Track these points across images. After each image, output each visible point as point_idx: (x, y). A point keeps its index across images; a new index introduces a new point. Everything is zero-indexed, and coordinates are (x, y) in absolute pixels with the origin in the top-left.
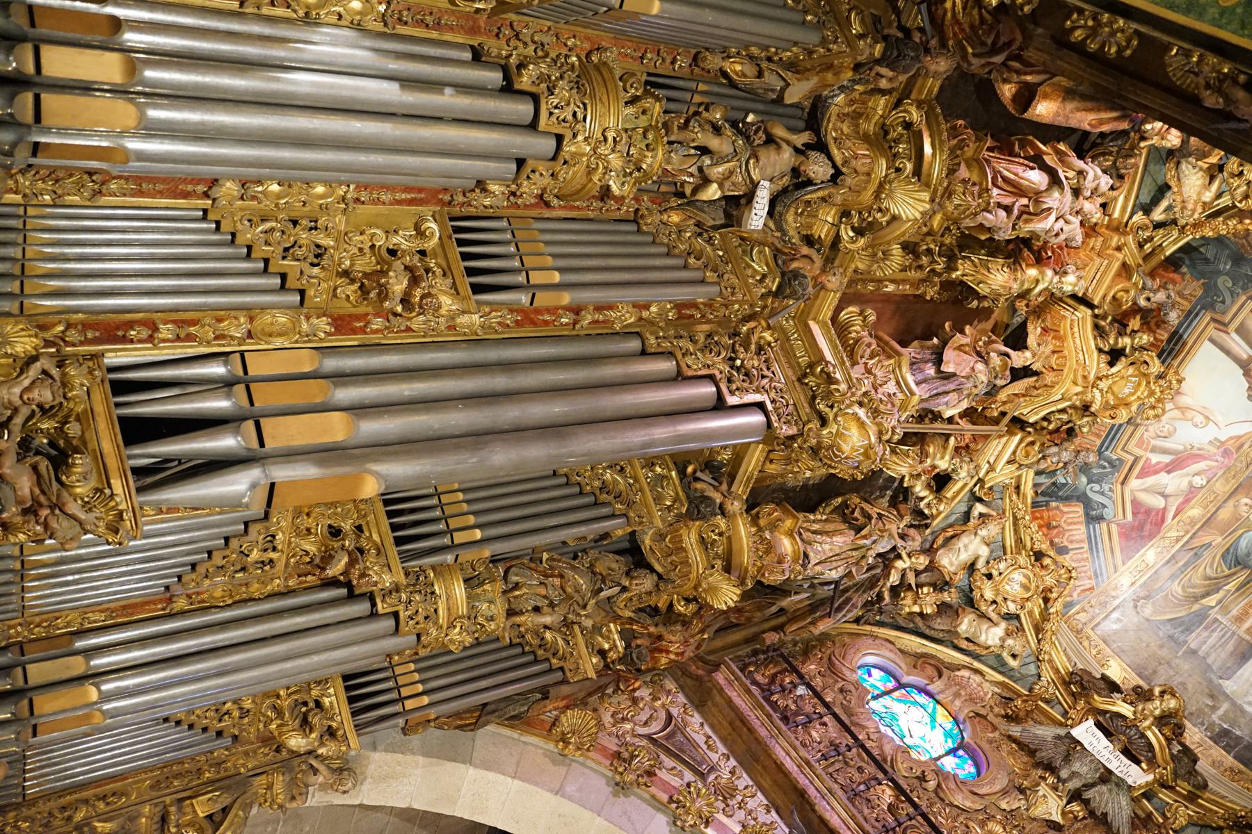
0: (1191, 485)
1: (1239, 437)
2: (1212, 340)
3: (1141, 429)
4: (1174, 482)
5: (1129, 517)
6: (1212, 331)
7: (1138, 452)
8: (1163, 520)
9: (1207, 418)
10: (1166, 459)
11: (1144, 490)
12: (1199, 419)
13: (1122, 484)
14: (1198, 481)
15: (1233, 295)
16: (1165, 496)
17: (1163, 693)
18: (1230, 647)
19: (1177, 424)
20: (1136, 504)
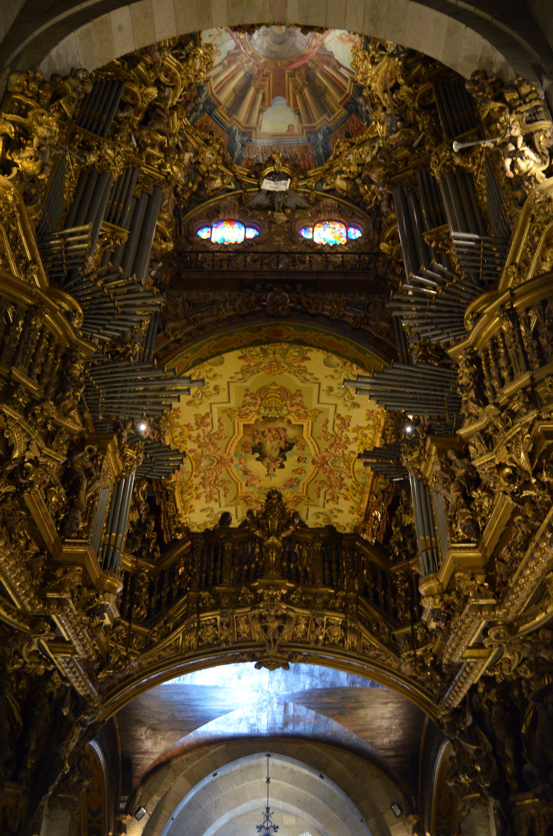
9: (341, 38)
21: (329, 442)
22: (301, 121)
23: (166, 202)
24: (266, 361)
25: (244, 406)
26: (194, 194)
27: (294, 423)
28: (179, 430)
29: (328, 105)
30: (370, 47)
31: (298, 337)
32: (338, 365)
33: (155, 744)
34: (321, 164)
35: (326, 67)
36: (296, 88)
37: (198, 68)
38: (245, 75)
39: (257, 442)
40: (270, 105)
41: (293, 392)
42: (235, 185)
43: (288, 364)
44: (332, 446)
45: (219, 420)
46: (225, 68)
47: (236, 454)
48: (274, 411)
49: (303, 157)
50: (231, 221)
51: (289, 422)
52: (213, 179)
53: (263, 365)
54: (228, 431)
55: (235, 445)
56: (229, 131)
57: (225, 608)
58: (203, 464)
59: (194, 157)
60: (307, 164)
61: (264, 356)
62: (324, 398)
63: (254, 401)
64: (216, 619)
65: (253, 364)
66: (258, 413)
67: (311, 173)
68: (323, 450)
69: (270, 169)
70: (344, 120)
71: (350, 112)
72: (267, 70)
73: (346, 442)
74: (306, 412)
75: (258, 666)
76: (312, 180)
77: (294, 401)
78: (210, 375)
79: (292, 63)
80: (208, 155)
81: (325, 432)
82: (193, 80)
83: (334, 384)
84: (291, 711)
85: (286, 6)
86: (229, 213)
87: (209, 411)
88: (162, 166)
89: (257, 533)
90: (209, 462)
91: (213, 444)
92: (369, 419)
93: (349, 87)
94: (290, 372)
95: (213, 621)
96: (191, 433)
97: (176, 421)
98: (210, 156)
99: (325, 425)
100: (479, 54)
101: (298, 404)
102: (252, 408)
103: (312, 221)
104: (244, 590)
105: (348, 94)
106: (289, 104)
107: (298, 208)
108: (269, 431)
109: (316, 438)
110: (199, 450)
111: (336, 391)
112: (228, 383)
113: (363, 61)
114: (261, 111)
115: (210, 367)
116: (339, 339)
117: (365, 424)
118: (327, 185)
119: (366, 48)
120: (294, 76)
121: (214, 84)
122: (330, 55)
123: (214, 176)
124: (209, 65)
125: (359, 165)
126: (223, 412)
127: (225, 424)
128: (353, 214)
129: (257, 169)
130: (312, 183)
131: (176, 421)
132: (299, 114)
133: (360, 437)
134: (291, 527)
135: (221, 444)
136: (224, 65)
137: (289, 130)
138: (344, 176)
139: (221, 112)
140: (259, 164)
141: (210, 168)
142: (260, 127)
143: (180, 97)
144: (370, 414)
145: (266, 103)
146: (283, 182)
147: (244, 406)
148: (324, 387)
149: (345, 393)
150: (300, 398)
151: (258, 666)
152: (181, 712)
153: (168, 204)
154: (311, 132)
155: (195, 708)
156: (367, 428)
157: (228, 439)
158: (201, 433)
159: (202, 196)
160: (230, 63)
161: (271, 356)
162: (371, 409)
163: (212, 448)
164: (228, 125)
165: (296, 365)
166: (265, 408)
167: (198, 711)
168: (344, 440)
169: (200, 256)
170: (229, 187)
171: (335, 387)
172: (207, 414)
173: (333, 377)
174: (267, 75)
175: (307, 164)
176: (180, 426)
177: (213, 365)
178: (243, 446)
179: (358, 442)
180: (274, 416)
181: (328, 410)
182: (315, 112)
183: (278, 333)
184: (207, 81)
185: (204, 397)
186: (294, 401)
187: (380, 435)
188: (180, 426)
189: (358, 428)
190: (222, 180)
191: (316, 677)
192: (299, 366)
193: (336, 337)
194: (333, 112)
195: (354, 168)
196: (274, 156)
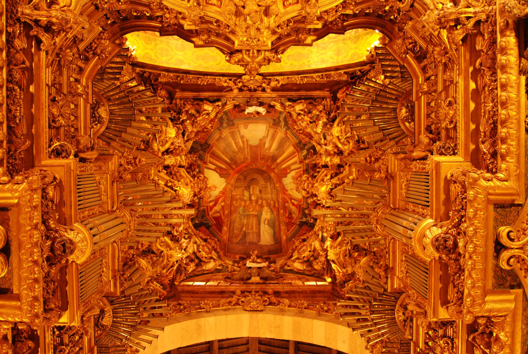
0: (222, 206)
1: (224, 188)
4: (217, 208)
5: (215, 222)
6: (205, 166)
7: (206, 205)
8: (222, 218)
9: (215, 187)
10: (213, 203)
11: (214, 213)
12: (214, 189)
13: (208, 214)
14: (223, 204)
15: (205, 155)
16: (218, 212)
17: (253, 252)
18: (255, 235)
19: (211, 193)
20: (214, 218)
35: (224, 167)
38: (276, 160)
40: (261, 140)
46: (289, 167)
52: (302, 110)
56: (288, 128)
71: (206, 143)
72: (262, 162)
79: (246, 166)
82: (310, 179)
93: (208, 158)
105: (208, 153)
106: (247, 141)
113: (201, 189)
116: (200, 65)
120: (244, 158)
121: (296, 159)
122: (221, 176)
129: (269, 110)
136: (289, 168)
137: (247, 126)
141: (302, 116)
142: (266, 128)
143: (319, 172)
145: (262, 142)
154: (231, 124)
160: (285, 169)
170: (290, 103)
184: (301, 162)
190: (294, 110)
194: (218, 140)
196: (257, 116)
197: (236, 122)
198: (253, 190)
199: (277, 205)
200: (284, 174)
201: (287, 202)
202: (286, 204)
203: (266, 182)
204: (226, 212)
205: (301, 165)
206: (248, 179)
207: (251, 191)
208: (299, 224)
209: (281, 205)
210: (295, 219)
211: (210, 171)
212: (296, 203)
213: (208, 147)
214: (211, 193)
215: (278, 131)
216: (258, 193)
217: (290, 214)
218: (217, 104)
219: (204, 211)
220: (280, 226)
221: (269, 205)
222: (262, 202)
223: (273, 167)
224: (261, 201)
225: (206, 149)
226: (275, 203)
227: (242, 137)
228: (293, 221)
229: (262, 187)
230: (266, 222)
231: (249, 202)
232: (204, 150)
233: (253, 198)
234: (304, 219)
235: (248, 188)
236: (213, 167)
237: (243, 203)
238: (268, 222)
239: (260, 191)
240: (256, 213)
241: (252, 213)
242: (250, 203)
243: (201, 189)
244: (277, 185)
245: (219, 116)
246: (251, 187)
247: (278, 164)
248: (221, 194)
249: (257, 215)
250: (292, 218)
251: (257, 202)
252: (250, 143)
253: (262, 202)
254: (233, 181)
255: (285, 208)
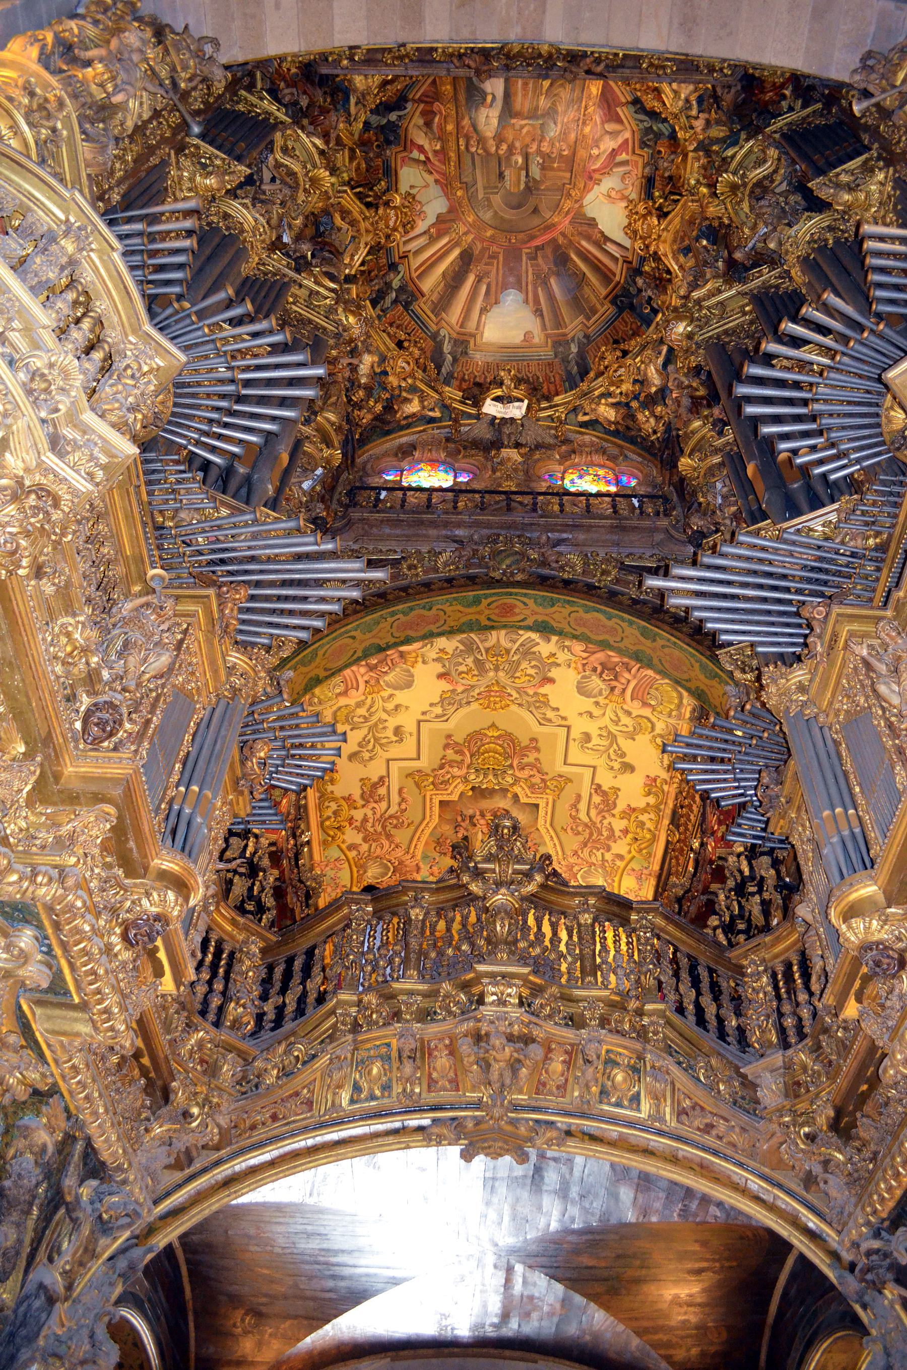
2: (627, 249)
3: (640, 175)
4: (609, 144)
5: (618, 109)
7: (635, 158)
10: (619, 159)
12: (613, 194)
14: (595, 152)
19: (622, 186)
20: (619, 121)
21: (581, 838)
22: (544, 327)
23: (333, 399)
24: (482, 684)
25: (442, 767)
26: (377, 418)
27: (523, 800)
28: (334, 806)
29: (587, 301)
30: (657, 194)
31: (540, 618)
32: (600, 694)
33: (260, 1344)
34: (573, 386)
35: (584, 243)
36: (537, 275)
37: (391, 224)
38: (462, 255)
39: (460, 835)
41: (525, 742)
42: (442, 413)
43: (518, 690)
44: (585, 845)
45: (400, 791)
46: (433, 240)
47: (425, 857)
48: (491, 777)
49: (547, 379)
50: (433, 463)
51: (516, 797)
52: (407, 400)
53: (477, 691)
54: (414, 814)
55: (424, 839)
56: (435, 336)
57: (407, 1021)
58: (369, 874)
59: (379, 365)
60: (552, 388)
61: (480, 675)
62: (576, 755)
63: (458, 758)
64: (388, 1045)
65: (460, 689)
66: (466, 780)
67: (558, 399)
68: (569, 853)
69: (498, 392)
70: (611, 322)
71: (621, 310)
72: (494, 248)
73: (608, 838)
74: (543, 781)
75: (467, 1156)
76: (561, 409)
77: (526, 760)
78: (390, 706)
79: (532, 238)
80: (401, 363)
81: (574, 818)
82: (383, 241)
83: (592, 728)
84: (518, 1287)
85: (544, 12)
86: (430, 450)
87: (384, 773)
88: (331, 310)
89: (474, 888)
90: (380, 870)
91: (389, 836)
92: (648, 794)
93: (619, 272)
94: (520, 705)
95: (384, 1050)
96: (353, 812)
97: (330, 788)
98: (404, 365)
99: (575, 806)
100: (872, 29)
101: (531, 766)
102: (455, 771)
103: (560, 464)
104: (446, 987)
105: (619, 283)
106: (526, 301)
107: (538, 446)
108: (483, 815)
109: (559, 829)
110: (365, 847)
111: (595, 740)
112: (419, 722)
113: (644, 216)
114: (484, 310)
115: (390, 691)
116: (610, 619)
117: (641, 803)
118: (585, 414)
119: (650, 196)
120: (535, 258)
121: (416, 262)
123: (410, 397)
124: (408, 225)
125: (635, 381)
126: (408, 776)
127: (410, 799)
128: (626, 456)
129: (476, 391)
130: (561, 412)
131: (330, 788)
132: (542, 315)
133: (632, 828)
134: (539, 878)
135: (401, 836)
136: (431, 237)
137: (525, 340)
138: (611, 400)
139: (423, 307)
140: (478, 385)
142: (482, 333)
143: (362, 264)
144: (651, 783)
145: (492, 300)
146: (517, 404)
147: (442, 767)
148: (575, 734)
149: (611, 745)
150: (536, 755)
151: (467, 1156)
152: (311, 1278)
153: (335, 404)
154: (560, 343)
155: (338, 1270)
156: (644, 811)
157: (413, 828)
158: (370, 813)
159: (389, 423)
160: (439, 236)
161: (492, 674)
162: (652, 775)
163: (386, 843)
164: (433, 328)
165: (531, 692)
166: (477, 770)
167: (343, 1278)
168: (605, 834)
169: (383, 494)
170: (431, 414)
171: (594, 733)
172: (381, 779)
173: (591, 715)
174: (494, 256)
175: (552, 388)
176: (334, 799)
177: (395, 688)
178: (438, 843)
179: (630, 836)
180: (491, 786)
181: (581, 776)
182: (565, 311)
183: (508, 610)
184: (405, 257)
185: (377, 746)
186: (526, 760)
187: (666, 822)
188: (334, 799)
189: (632, 810)
190: (421, 401)
191: (573, 1202)
192: (536, 694)
193: (604, 612)
194: (594, 311)
195: (626, 387)
196: (502, 374)
197: (548, 353)
198: (519, 180)
199: (462, 142)
200: (444, 222)
201: (436, 152)
202: (438, 147)
203: (488, 200)
204: (587, 130)
205: (403, 249)
206: (529, 207)
207: (523, 178)
208: (406, 101)
209: (452, 145)
210: (418, 113)
211: (618, 241)
212: (415, 154)
213: (616, 297)
214: (622, 186)
215: (457, 328)
216: (507, 173)
217: (428, 124)
218: (586, 418)
219: (643, 144)
220: (455, 89)
221: (482, 140)
222: (498, 148)
223: (470, 238)
224: (501, 152)
225: (622, 296)
226: (467, 148)
227: (538, 312)
228: (422, 106)
229: (496, 187)
230: (489, 98)
231: (530, 150)
232: (626, 293)
233: (520, 160)
234: (393, 117)
235: (531, 188)
236: (610, 247)
237: (545, 147)
238: (485, 100)
239: (501, 176)
240: (514, 121)
241: (523, 122)
242: (527, 146)
243: (644, 216)
244: (459, 193)
245: (584, 386)
246: (522, 187)
247: (457, 244)
248: (596, 176)
249: (511, 117)
250: (423, 113)
251: (511, 149)
252: (520, 297)
253: (498, 148)
254: (567, 205)
255: (442, 137)
